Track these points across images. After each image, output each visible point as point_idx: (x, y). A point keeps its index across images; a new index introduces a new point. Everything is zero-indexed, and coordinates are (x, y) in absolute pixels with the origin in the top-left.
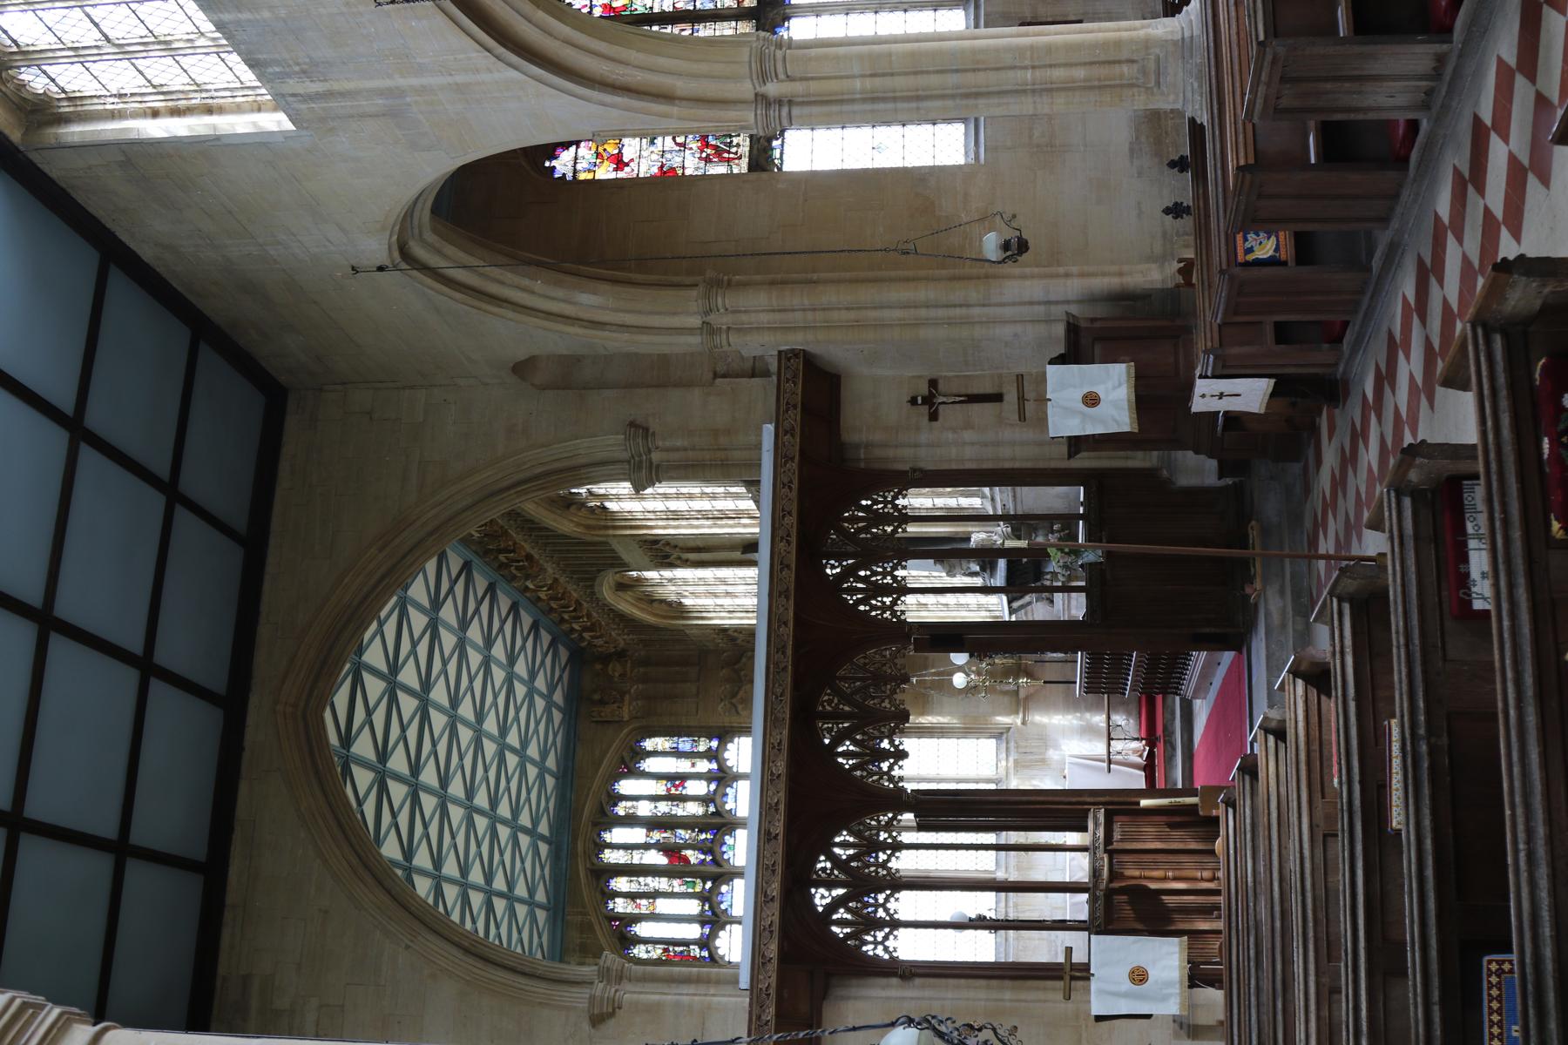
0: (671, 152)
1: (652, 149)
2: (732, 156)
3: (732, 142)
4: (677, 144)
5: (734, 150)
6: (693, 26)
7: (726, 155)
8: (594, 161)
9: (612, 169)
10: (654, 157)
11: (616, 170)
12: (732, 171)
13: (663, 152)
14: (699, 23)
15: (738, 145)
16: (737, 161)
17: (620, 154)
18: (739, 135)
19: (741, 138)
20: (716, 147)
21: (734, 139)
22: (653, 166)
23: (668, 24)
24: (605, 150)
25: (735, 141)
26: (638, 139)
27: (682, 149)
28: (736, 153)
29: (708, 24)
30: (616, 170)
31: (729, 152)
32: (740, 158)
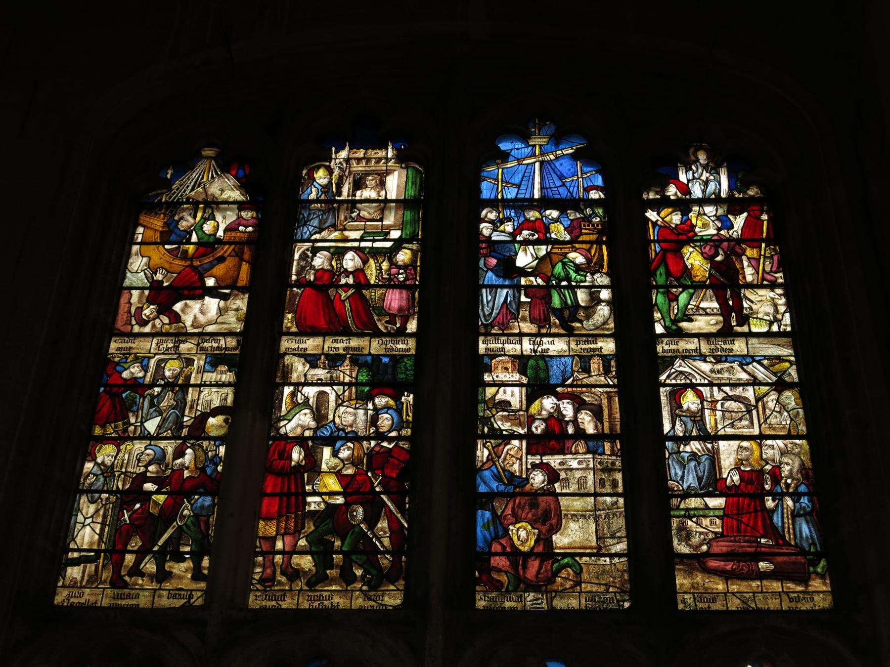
0: (181, 405)
1: (199, 361)
2: (130, 558)
3: (179, 558)
4: (202, 419)
5: (150, 567)
6: (611, 437)
7: (135, 543)
8: (194, 238)
9: (159, 277)
10: (171, 369)
11: (156, 286)
12: (75, 562)
13: (186, 386)
14: (626, 454)
15: (163, 576)
16: (106, 575)
17: (201, 292)
18: (197, 575)
19: (187, 583)
20: (169, 513)
21: (189, 564)
22: (145, 369)
23: (617, 376)
24: (221, 260)
25: (181, 568)
26: (238, 327)
27: (185, 432)
28: (136, 571)
29: (619, 476)
30: (156, 286)
31: (141, 554)
32: (117, 582)
